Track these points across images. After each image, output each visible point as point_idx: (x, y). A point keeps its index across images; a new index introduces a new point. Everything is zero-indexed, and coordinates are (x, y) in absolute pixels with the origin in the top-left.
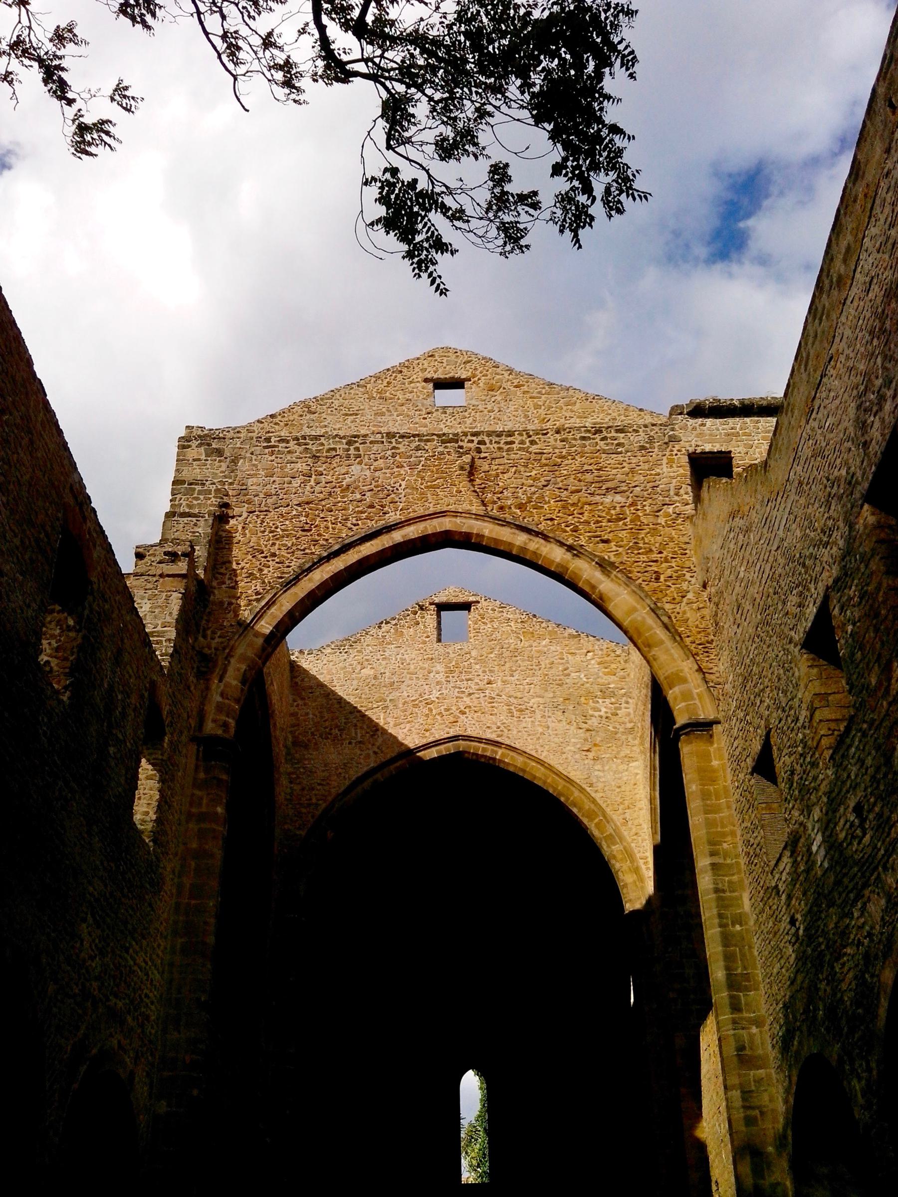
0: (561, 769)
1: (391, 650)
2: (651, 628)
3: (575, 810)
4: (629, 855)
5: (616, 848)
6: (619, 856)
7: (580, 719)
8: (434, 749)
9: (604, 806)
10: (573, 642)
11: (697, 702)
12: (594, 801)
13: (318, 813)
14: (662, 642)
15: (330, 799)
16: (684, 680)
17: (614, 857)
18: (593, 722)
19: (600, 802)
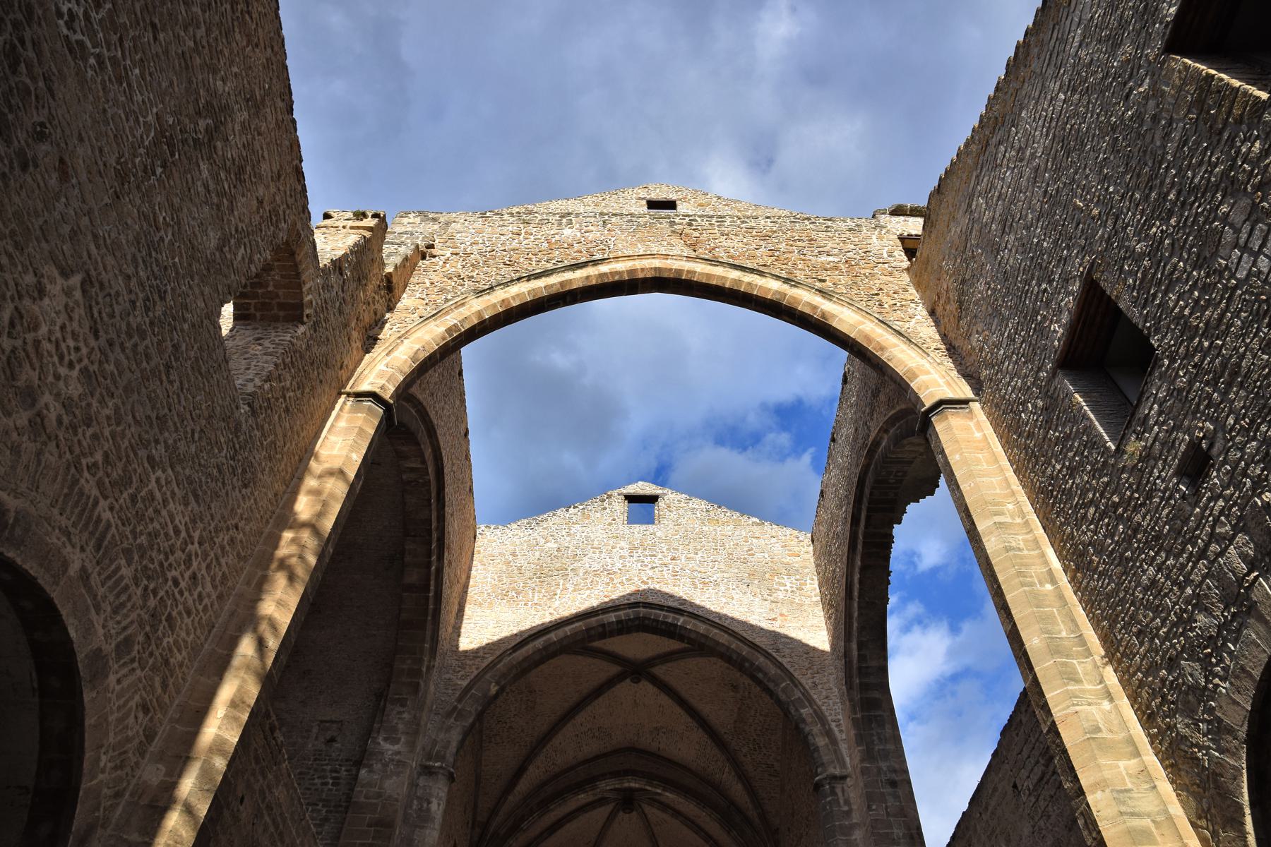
0: (745, 635)
1: (576, 528)
2: (881, 336)
3: (760, 675)
4: (820, 718)
5: (805, 711)
6: (809, 720)
7: (765, 593)
8: (613, 614)
9: (791, 670)
10: (755, 528)
11: (945, 388)
12: (780, 666)
13: (484, 665)
14: (896, 346)
15: (498, 653)
16: (928, 373)
17: (804, 721)
18: (781, 595)
19: (788, 667)
